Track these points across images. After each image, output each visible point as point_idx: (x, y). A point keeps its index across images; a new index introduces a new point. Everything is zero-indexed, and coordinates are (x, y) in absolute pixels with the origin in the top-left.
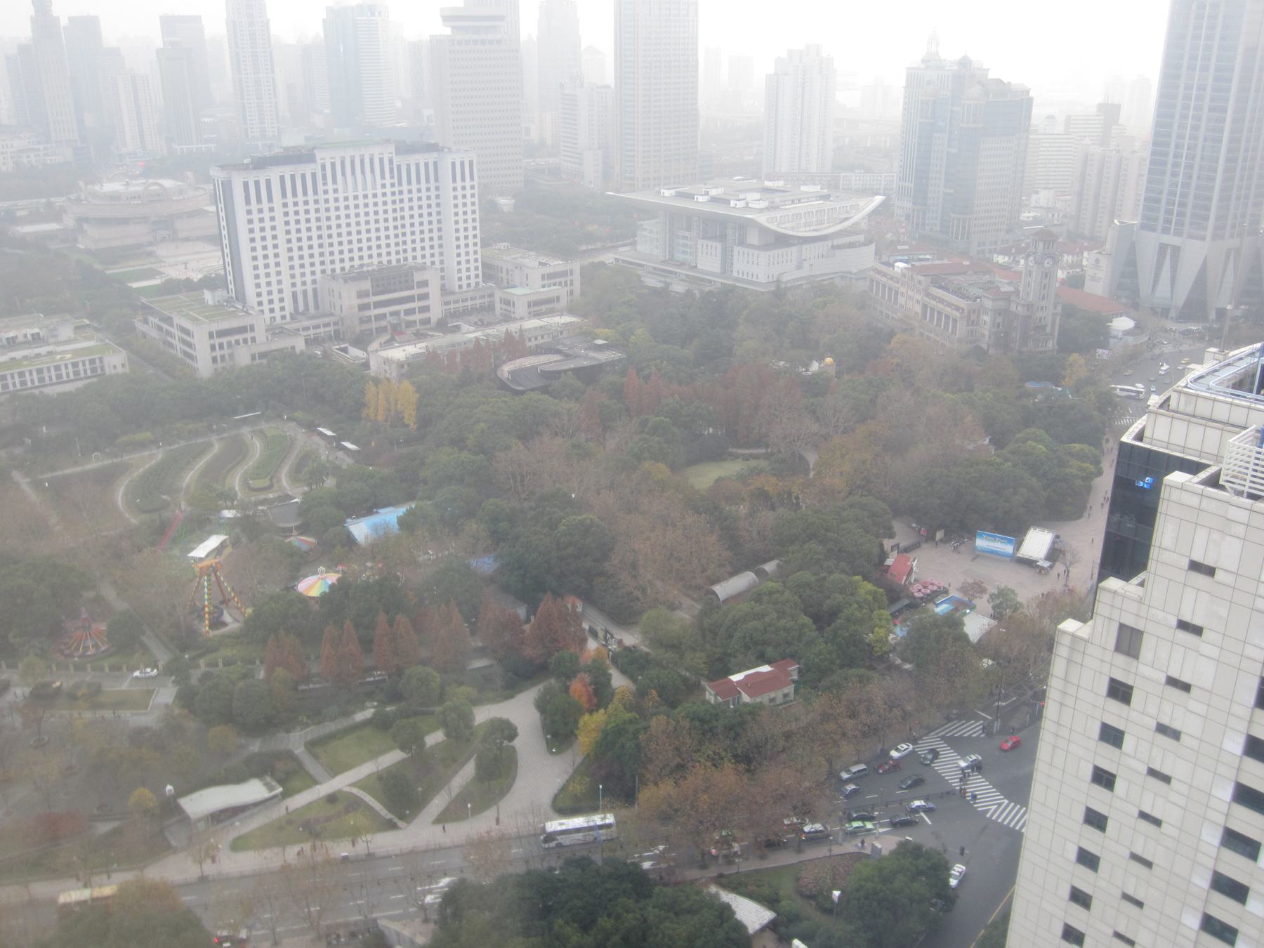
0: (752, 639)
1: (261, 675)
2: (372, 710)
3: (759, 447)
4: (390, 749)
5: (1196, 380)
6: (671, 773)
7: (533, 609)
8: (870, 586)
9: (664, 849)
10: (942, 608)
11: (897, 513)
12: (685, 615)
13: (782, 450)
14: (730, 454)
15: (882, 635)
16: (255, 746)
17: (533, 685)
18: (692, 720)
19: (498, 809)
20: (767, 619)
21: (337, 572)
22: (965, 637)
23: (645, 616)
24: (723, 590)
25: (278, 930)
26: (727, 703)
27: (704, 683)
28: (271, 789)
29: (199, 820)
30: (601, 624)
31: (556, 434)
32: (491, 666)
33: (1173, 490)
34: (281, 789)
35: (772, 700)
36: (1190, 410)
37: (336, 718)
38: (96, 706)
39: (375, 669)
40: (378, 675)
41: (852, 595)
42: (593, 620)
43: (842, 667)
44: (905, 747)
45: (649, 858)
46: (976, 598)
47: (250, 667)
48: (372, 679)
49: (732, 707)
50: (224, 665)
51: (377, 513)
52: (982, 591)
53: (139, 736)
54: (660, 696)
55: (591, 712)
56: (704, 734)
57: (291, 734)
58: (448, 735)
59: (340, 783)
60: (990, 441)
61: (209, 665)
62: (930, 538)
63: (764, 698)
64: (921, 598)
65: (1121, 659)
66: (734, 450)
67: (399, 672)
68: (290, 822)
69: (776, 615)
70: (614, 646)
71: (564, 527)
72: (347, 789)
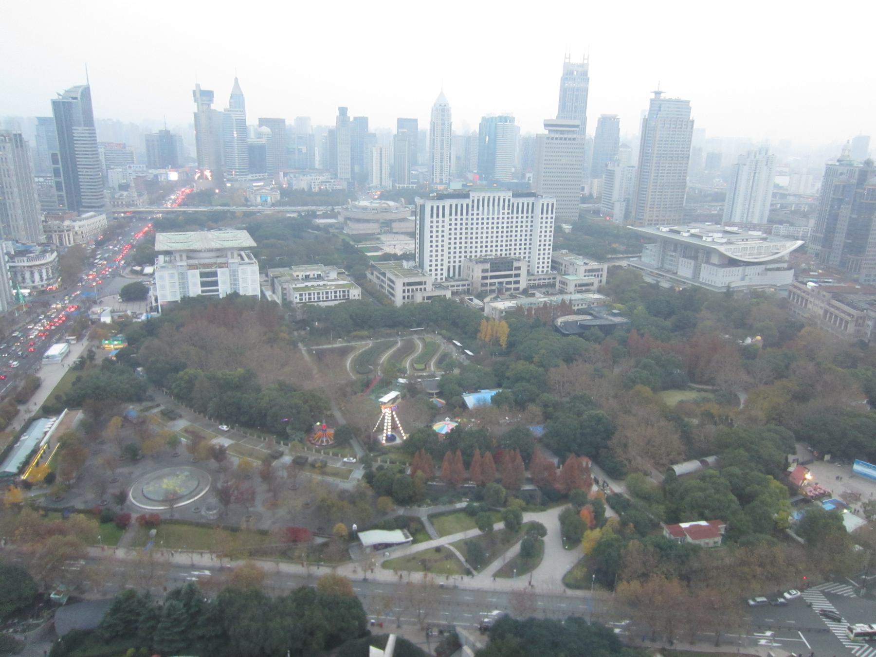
1: (409, 472)
2: (466, 504)
3: (708, 385)
6: (639, 577)
7: (563, 461)
8: (778, 483)
9: (629, 623)
10: (828, 507)
11: (800, 438)
12: (654, 480)
13: (723, 389)
14: (690, 387)
16: (401, 511)
17: (558, 505)
19: (531, 576)
20: (707, 492)
21: (456, 422)
23: (629, 477)
24: (680, 469)
25: (402, 619)
26: (677, 540)
27: (662, 524)
28: (407, 537)
29: (368, 547)
30: (602, 477)
31: (586, 361)
32: (535, 490)
34: (411, 539)
35: (707, 544)
38: (324, 473)
39: (470, 479)
40: (471, 484)
41: (765, 487)
42: (596, 473)
43: (755, 531)
44: (795, 592)
45: (618, 627)
46: (852, 503)
47: (403, 466)
48: (467, 485)
49: (679, 543)
50: (390, 463)
51: (480, 392)
53: (343, 495)
54: (635, 527)
56: (662, 557)
59: (443, 541)
60: (868, 402)
62: (821, 458)
63: (702, 542)
64: (812, 497)
66: (692, 385)
67: (483, 485)
68: (414, 558)
69: (713, 491)
70: (608, 492)
72: (447, 546)
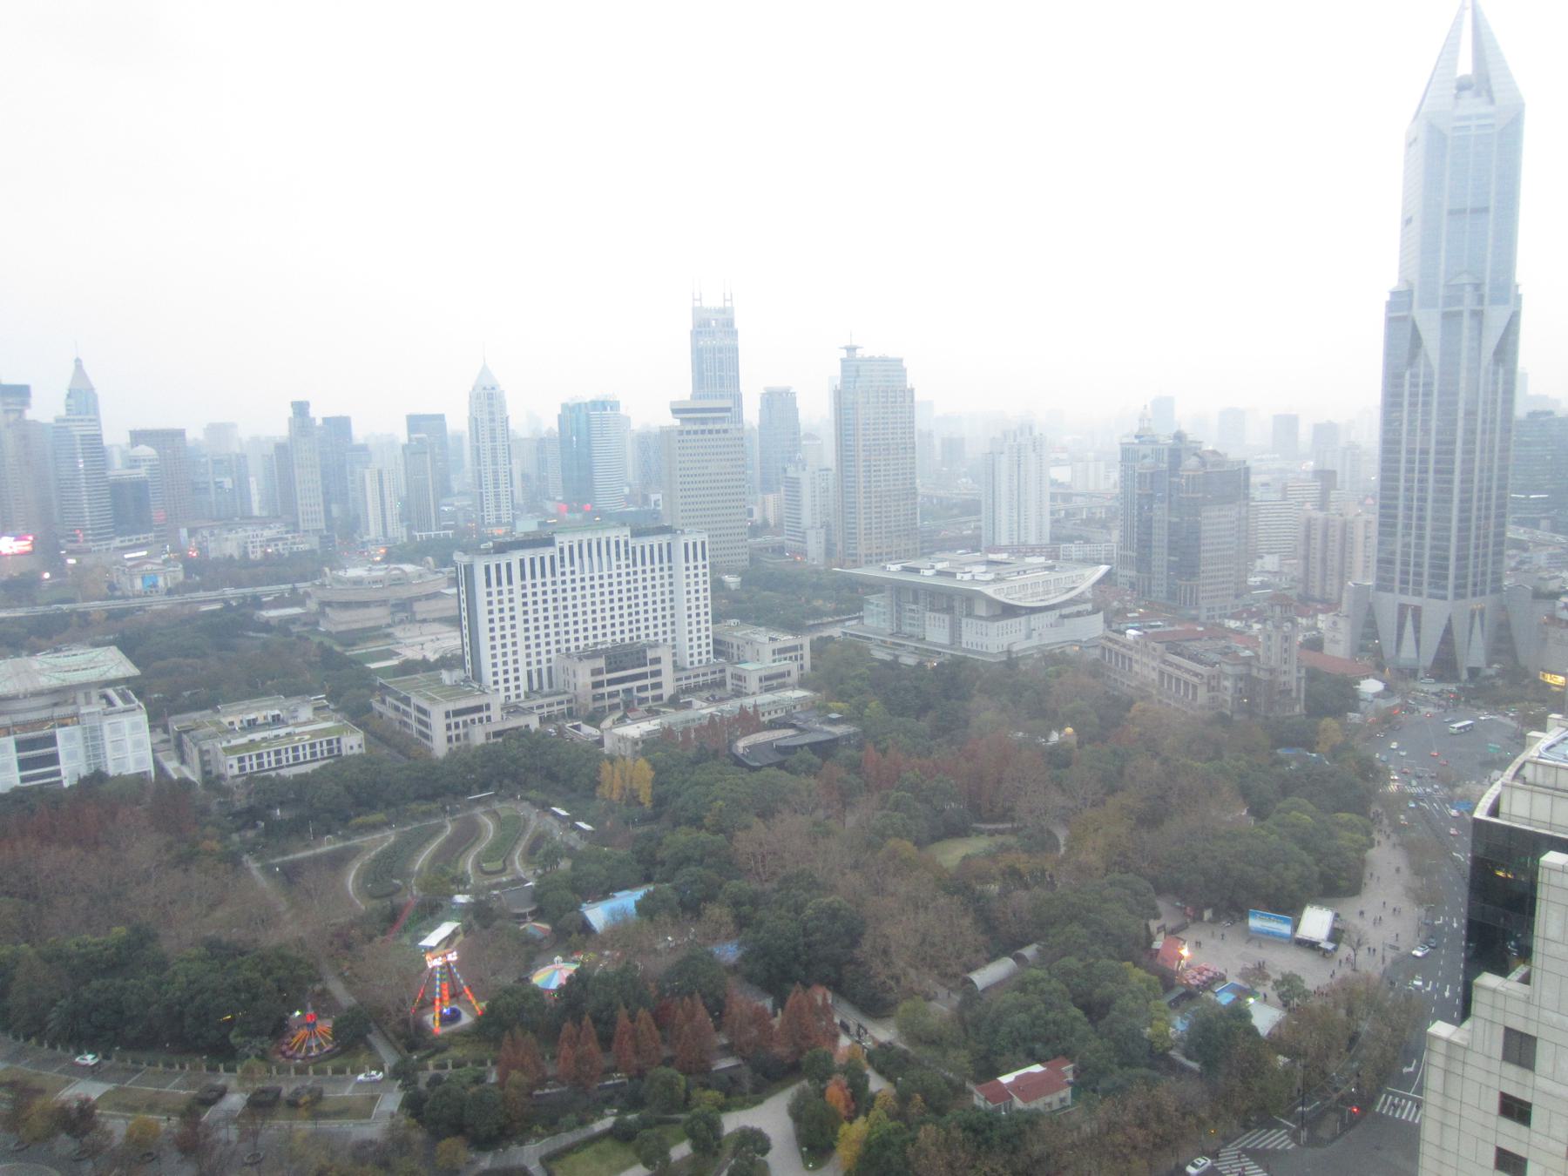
0: (1020, 1034)
1: (493, 1077)
3: (1002, 822)
4: (632, 1164)
5: (1548, 748)
7: (780, 1002)
8: (1141, 973)
10: (1225, 999)
11: (1160, 891)
12: (942, 1007)
14: (975, 830)
15: (1163, 1029)
17: (784, 1087)
18: (964, 1130)
20: (1034, 1011)
21: (575, 962)
22: (1253, 1031)
23: (901, 1008)
24: (984, 977)
26: (998, 1110)
27: (970, 1085)
30: (854, 1019)
31: (796, 812)
32: (739, 1066)
33: (1553, 873)
35: (1050, 1105)
36: (1550, 781)
37: (574, 1127)
38: (317, 1115)
39: (615, 1070)
40: (618, 1078)
41: (1123, 983)
42: (845, 1013)
44: (1203, 1161)
46: (1259, 985)
48: (611, 1082)
50: (454, 1067)
51: (614, 897)
52: (1266, 977)
53: (362, 1153)
54: (925, 1101)
55: (851, 1120)
56: (979, 1147)
57: (525, 1147)
58: (695, 1147)
61: (437, 1067)
62: (1198, 918)
63: (1039, 1104)
64: (1198, 986)
65: (1512, 1071)
67: (641, 1074)
69: (1043, 1006)
70: (869, 1044)
71: (810, 911)
